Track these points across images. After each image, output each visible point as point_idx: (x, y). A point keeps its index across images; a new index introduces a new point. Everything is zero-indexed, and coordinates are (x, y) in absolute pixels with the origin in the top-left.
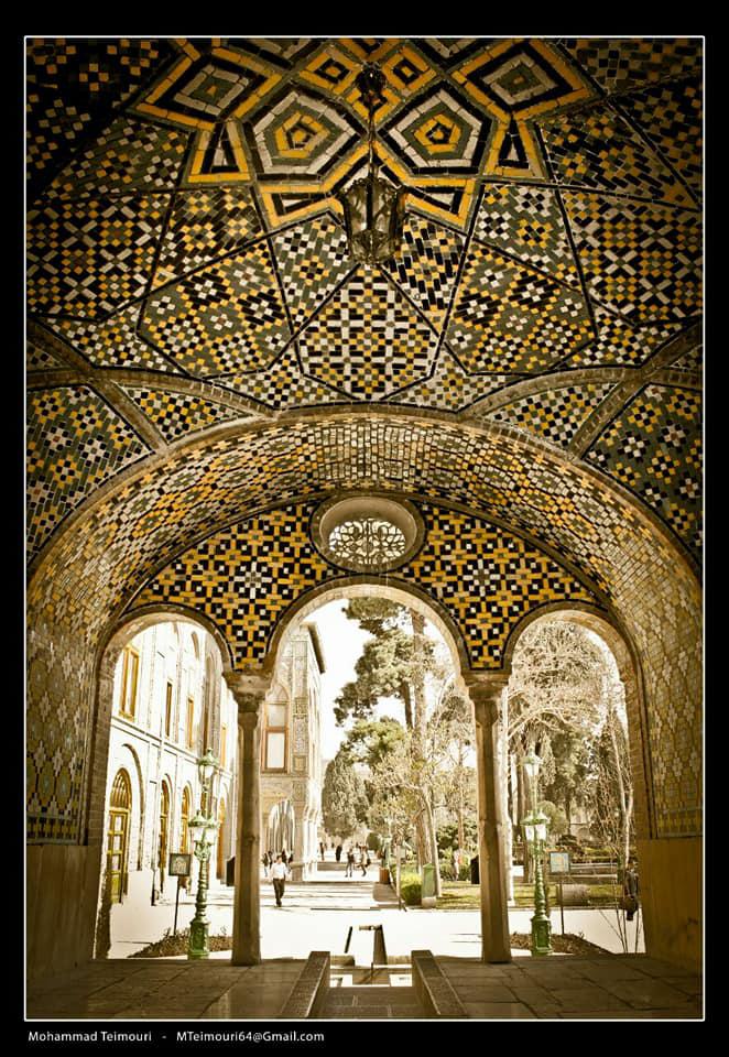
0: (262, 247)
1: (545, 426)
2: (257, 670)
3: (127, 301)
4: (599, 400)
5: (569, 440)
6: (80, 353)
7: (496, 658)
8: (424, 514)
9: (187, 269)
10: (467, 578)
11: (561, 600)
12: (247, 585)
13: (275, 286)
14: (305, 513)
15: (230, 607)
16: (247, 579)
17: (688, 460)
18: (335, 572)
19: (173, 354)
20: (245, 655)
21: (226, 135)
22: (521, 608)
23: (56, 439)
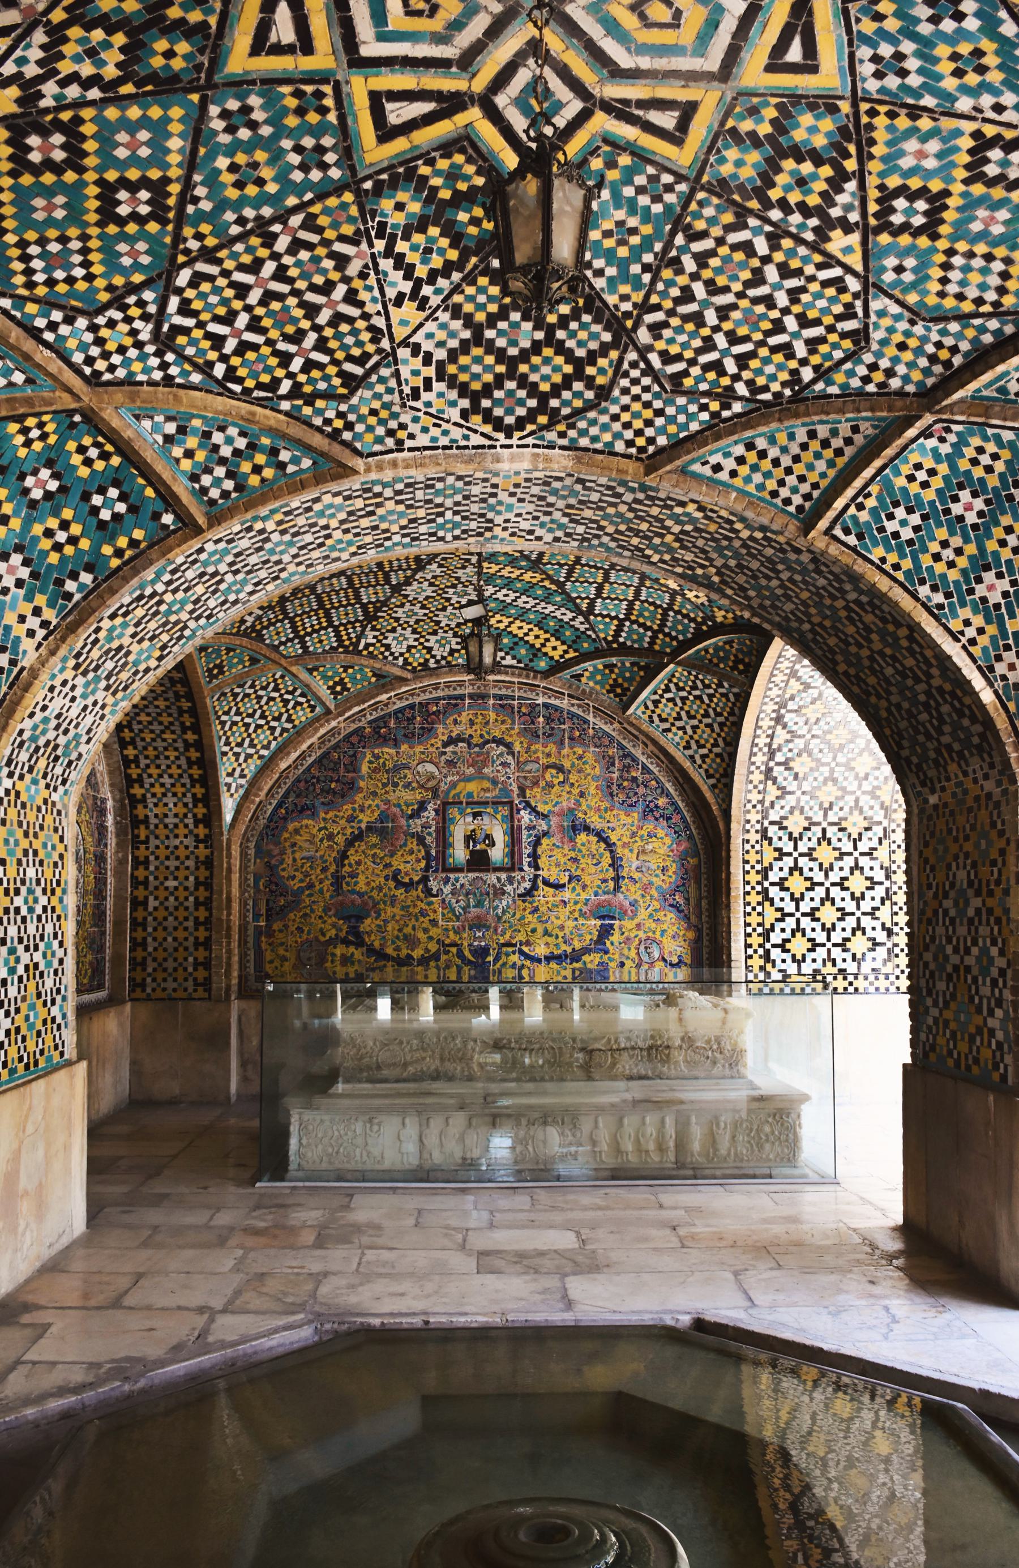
0: (872, 113)
3: (858, 303)
6: (888, 394)
9: (854, 217)
13: (969, 127)
19: (996, 304)
21: (626, 102)
23: (969, 508)
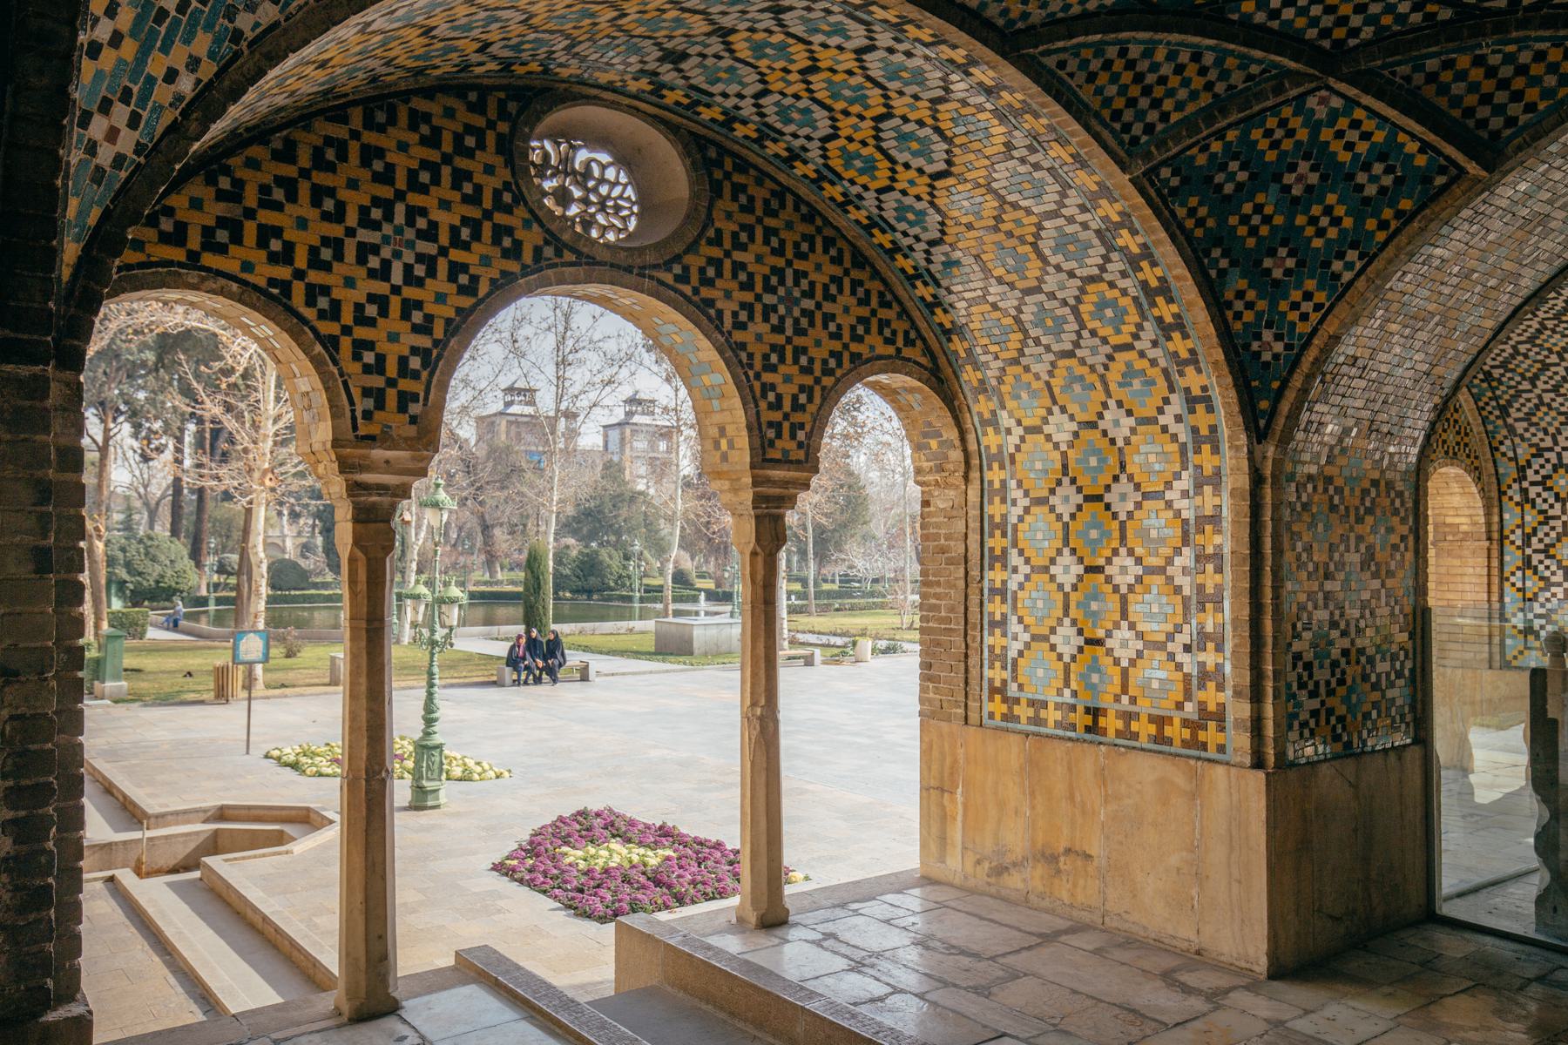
1: (1119, 103)
2: (406, 439)
4: (1230, 87)
5: (1144, 139)
7: (800, 445)
8: (710, 165)
10: (769, 299)
11: (890, 357)
12: (386, 252)
14: (503, 114)
15: (350, 298)
16: (386, 240)
17: (1300, 220)
18: (559, 253)
20: (380, 405)
22: (840, 365)
